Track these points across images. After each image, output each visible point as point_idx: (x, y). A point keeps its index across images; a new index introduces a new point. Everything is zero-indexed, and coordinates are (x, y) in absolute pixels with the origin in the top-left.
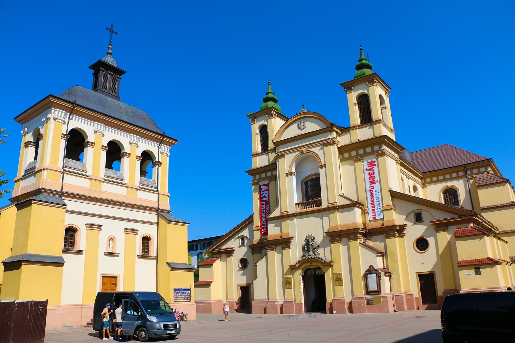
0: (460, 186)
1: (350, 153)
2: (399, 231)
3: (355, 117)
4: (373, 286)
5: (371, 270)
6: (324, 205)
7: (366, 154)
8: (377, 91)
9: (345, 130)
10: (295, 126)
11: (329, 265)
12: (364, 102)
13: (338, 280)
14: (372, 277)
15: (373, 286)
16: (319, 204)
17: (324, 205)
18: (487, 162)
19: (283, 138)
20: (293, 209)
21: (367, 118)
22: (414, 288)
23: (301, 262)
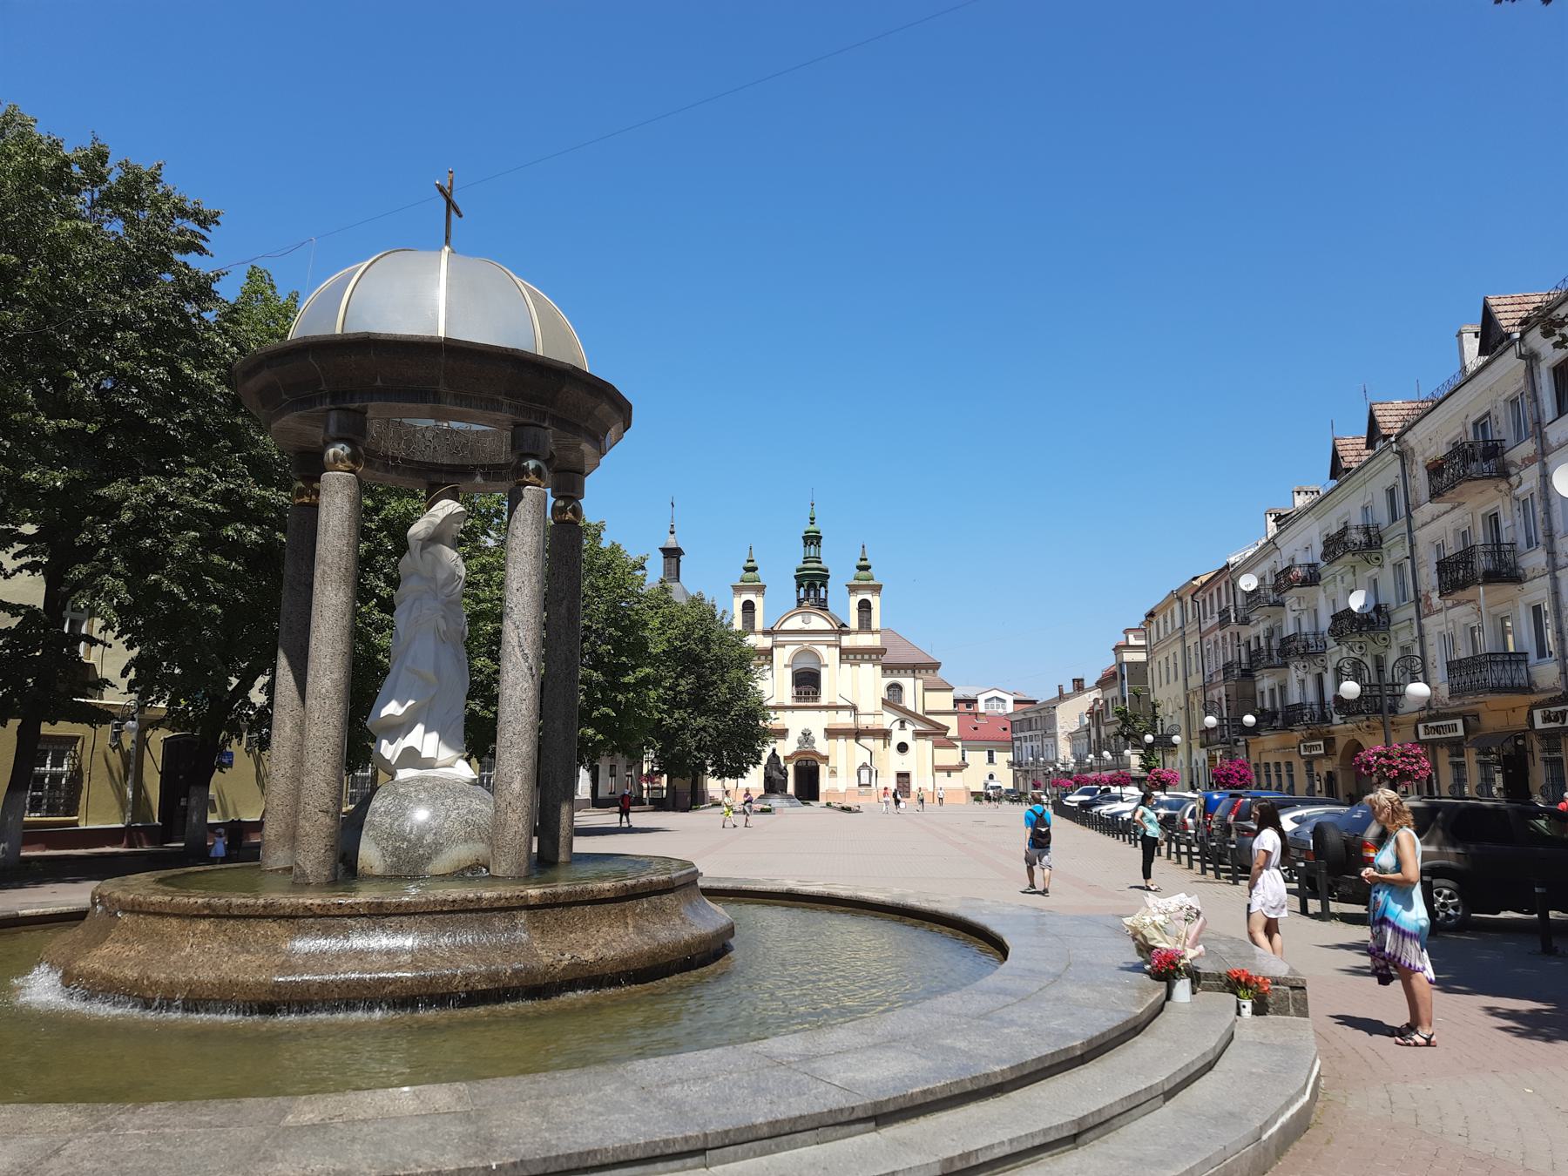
0: (907, 682)
1: (850, 656)
2: (885, 734)
3: (854, 623)
4: (865, 780)
5: (864, 766)
6: (823, 701)
7: (864, 661)
8: (875, 601)
9: (848, 633)
10: (799, 618)
11: (826, 759)
12: (865, 606)
13: (833, 773)
14: (865, 773)
15: (865, 780)
16: (816, 699)
17: (823, 701)
18: (935, 666)
19: (785, 627)
20: (789, 702)
21: (865, 626)
22: (893, 786)
23: (796, 754)
